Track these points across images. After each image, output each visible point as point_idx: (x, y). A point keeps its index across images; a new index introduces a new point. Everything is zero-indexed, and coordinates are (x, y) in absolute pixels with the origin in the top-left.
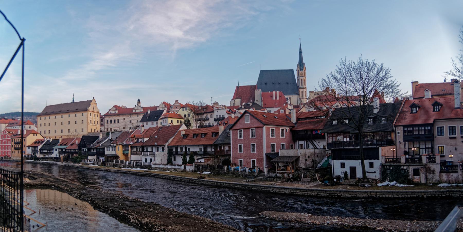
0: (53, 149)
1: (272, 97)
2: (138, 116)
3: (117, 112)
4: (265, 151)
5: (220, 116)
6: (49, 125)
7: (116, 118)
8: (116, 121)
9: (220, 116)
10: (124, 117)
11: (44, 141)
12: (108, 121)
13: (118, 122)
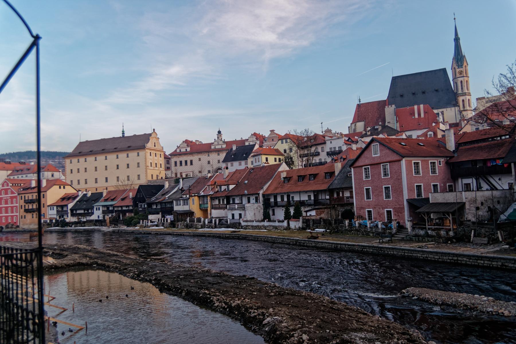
0: (93, 208)
2: (219, 155)
3: (189, 149)
4: (406, 197)
5: (335, 148)
7: (188, 158)
8: (189, 163)
9: (335, 148)
10: (200, 156)
11: (78, 196)
12: (176, 163)
13: (191, 163)
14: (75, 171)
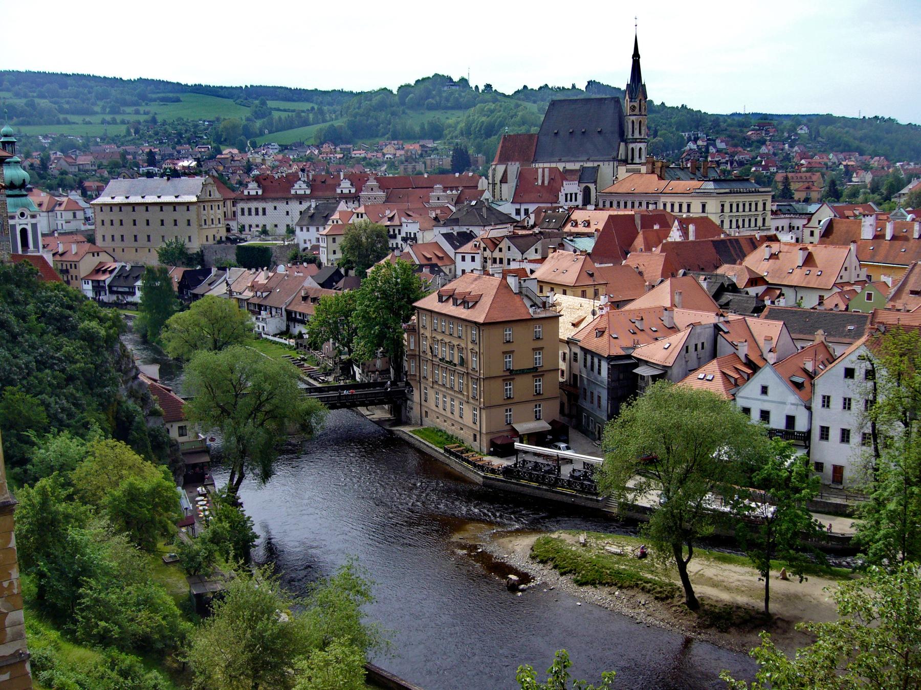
1: (536, 179)
2: (301, 203)
3: (260, 192)
6: (121, 224)
7: (260, 205)
12: (243, 210)
13: (264, 214)
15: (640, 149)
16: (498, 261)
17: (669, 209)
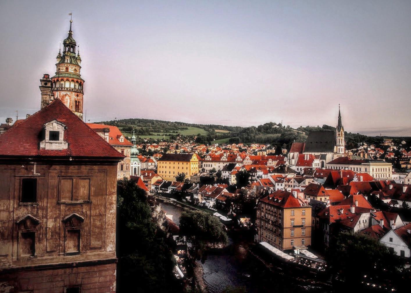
0: (168, 188)
2: (224, 163)
3: (211, 159)
6: (166, 168)
7: (210, 163)
11: (163, 182)
12: (205, 165)
14: (161, 167)
15: (342, 149)
16: (290, 186)
17: (353, 170)
